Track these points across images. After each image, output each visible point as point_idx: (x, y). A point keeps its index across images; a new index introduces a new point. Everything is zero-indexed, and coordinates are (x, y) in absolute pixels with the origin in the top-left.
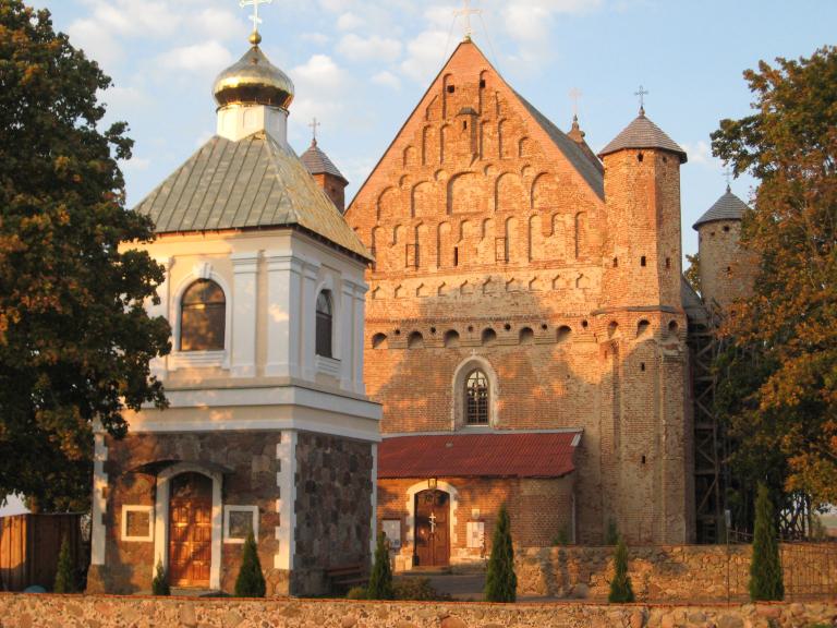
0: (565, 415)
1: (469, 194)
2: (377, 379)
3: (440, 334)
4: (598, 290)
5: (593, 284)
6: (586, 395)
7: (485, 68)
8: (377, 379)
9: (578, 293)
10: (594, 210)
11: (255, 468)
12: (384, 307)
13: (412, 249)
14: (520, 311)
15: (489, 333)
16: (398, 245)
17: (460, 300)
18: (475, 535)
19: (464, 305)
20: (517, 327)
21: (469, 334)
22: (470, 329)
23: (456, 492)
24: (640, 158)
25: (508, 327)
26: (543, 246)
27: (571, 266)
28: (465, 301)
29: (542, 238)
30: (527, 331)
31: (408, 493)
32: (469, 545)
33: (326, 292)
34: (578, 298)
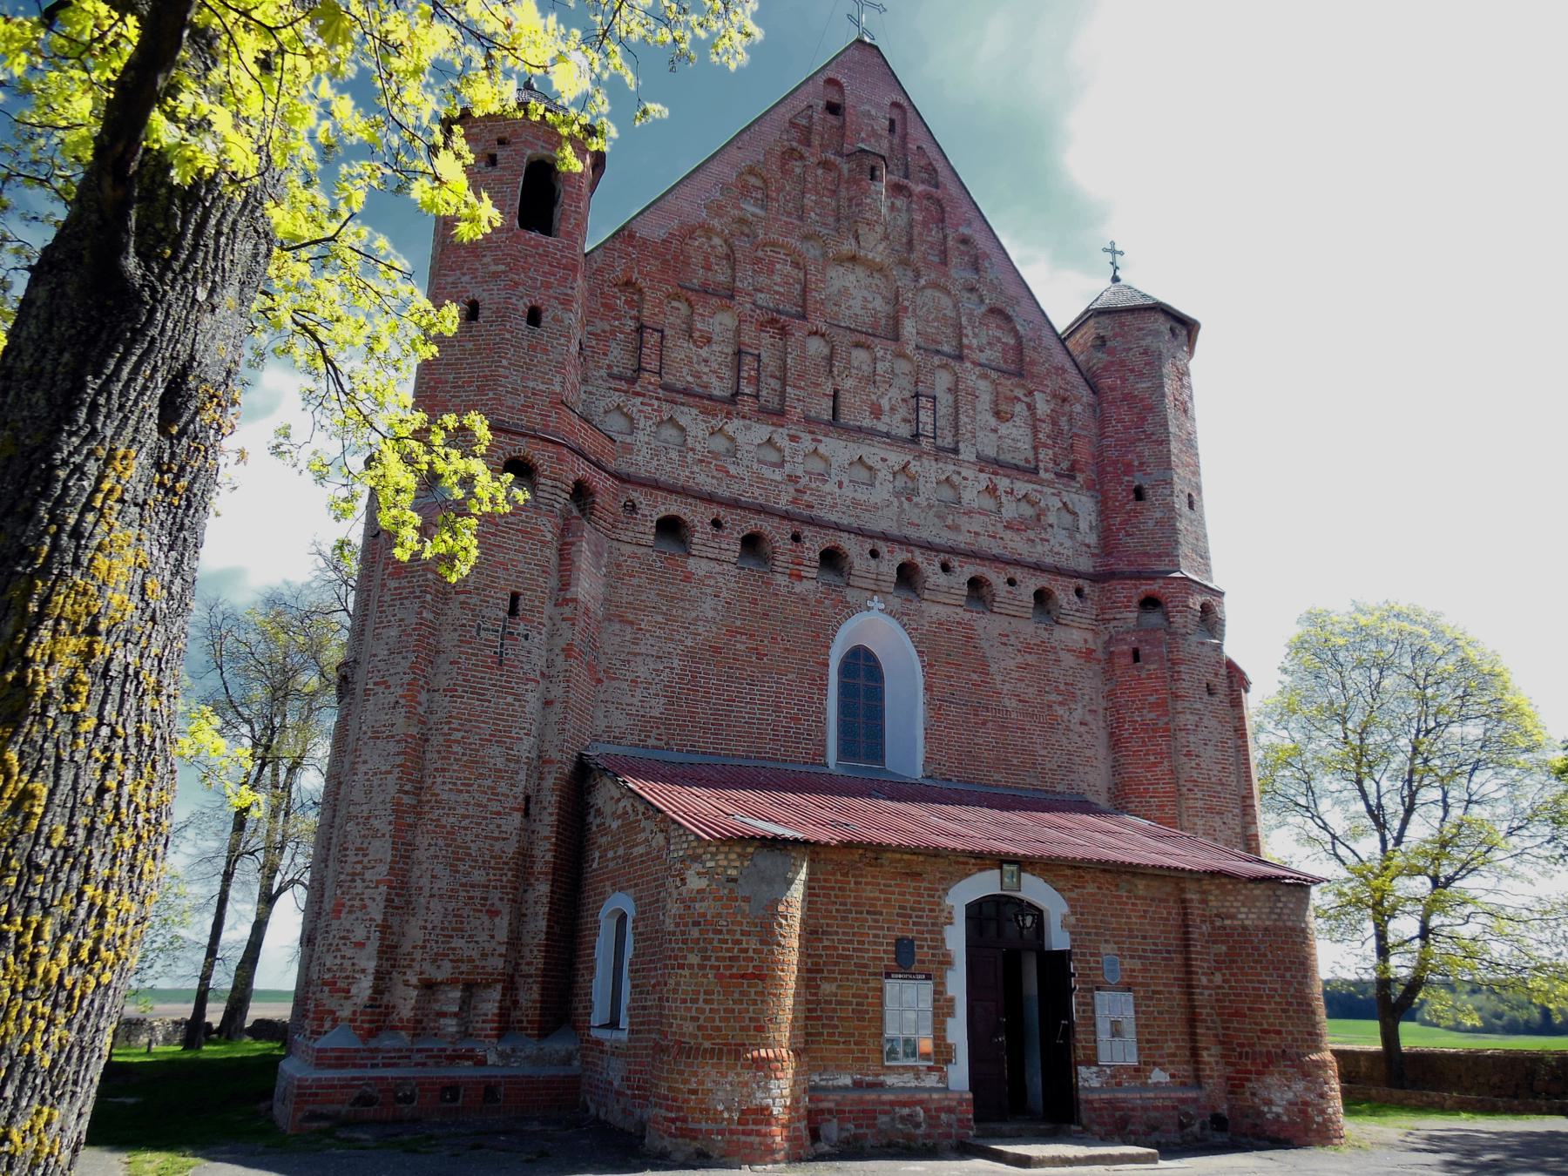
2: (660, 619)
4: (1092, 539)
8: (660, 619)
12: (684, 464)
15: (907, 576)
16: (715, 347)
17: (848, 491)
18: (1116, 1031)
19: (856, 503)
21: (873, 562)
23: (1065, 909)
25: (945, 568)
26: (993, 436)
27: (1050, 484)
28: (858, 496)
29: (993, 422)
31: (949, 901)
32: (1104, 1059)
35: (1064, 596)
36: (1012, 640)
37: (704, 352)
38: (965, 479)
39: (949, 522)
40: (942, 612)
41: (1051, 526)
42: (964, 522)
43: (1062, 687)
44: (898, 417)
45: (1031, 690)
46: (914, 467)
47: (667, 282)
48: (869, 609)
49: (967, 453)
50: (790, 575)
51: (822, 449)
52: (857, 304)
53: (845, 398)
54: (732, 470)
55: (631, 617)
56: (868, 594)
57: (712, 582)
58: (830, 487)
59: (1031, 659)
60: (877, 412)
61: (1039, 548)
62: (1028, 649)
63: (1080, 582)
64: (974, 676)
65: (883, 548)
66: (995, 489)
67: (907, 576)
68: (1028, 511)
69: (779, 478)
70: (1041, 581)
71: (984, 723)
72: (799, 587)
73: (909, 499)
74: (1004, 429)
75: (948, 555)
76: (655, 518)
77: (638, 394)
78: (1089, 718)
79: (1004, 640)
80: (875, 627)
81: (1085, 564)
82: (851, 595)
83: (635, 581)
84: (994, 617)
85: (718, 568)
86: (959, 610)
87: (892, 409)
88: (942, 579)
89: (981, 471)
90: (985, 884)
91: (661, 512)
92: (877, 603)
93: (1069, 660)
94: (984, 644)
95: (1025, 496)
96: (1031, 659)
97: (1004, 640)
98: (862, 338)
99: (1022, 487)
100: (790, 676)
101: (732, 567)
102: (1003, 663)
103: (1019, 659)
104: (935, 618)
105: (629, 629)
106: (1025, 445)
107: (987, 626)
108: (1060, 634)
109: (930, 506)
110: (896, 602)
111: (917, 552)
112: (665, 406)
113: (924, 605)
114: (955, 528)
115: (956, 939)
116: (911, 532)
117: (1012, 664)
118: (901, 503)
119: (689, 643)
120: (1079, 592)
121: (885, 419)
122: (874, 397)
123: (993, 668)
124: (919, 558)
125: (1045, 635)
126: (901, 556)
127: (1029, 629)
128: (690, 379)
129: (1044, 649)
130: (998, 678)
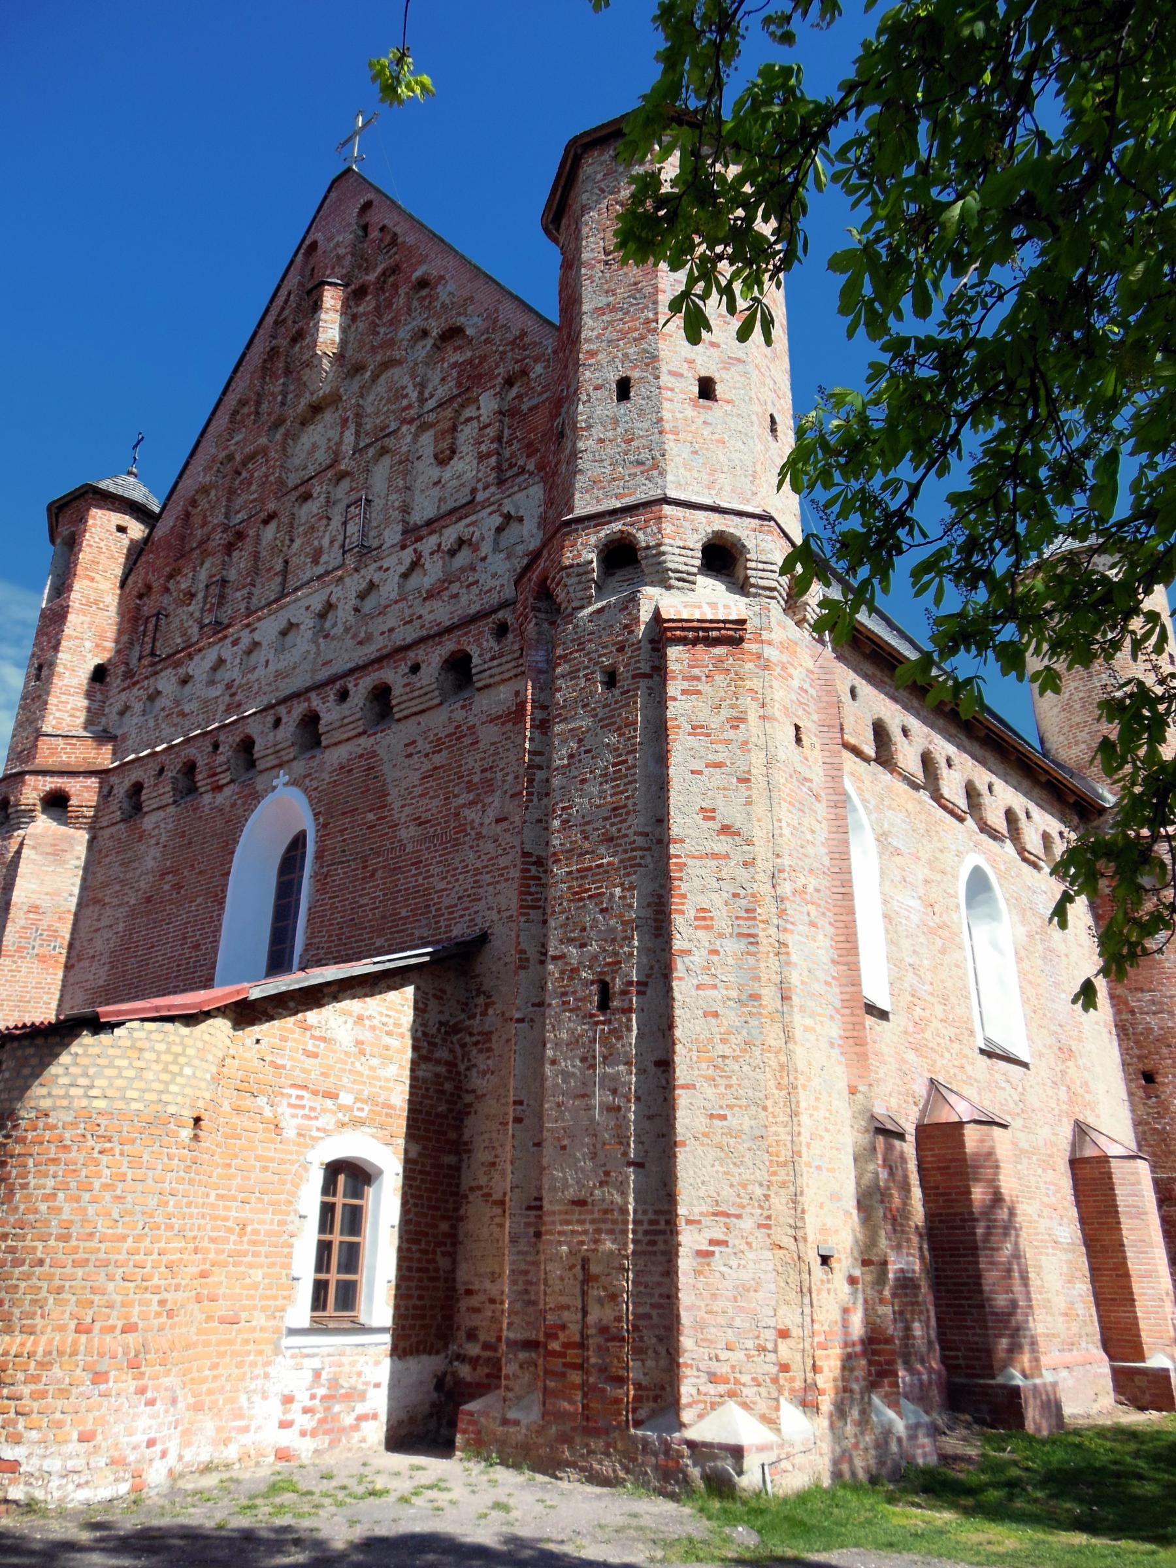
0: (447, 902)
1: (322, 450)
6: (499, 828)
7: (370, 196)
8: (118, 888)
10: (536, 360)
13: (215, 590)
14: (371, 650)
19: (279, 674)
22: (277, 723)
26: (436, 492)
27: (487, 503)
29: (435, 472)
34: (494, 576)
35: (480, 648)
36: (420, 743)
37: (191, 608)
38: (388, 569)
39: (362, 635)
41: (484, 559)
42: (379, 626)
43: (476, 779)
44: (337, 545)
45: (436, 802)
46: (337, 592)
47: (167, 565)
48: (274, 788)
50: (213, 790)
51: (257, 637)
53: (294, 561)
54: (187, 710)
55: (100, 895)
56: (274, 772)
57: (156, 832)
58: (260, 672)
59: (438, 759)
61: (464, 600)
62: (438, 745)
63: (500, 614)
64: (371, 816)
65: (282, 710)
66: (420, 557)
69: (219, 693)
70: (449, 645)
71: (375, 870)
72: (220, 799)
73: (326, 637)
74: (447, 475)
76: (122, 791)
77: (134, 684)
78: (511, 807)
79: (410, 750)
82: (260, 783)
83: (108, 860)
84: (401, 726)
85: (161, 814)
86: (362, 740)
87: (332, 542)
89: (404, 547)
91: (127, 784)
92: (283, 777)
94: (386, 768)
95: (461, 542)
96: (438, 759)
97: (410, 750)
98: (302, 489)
99: (450, 535)
100: (199, 900)
101: (172, 809)
102: (402, 777)
103: (427, 766)
104: (336, 766)
105: (97, 907)
109: (347, 630)
110: (299, 767)
111: (313, 695)
112: (152, 680)
113: (328, 752)
114: (369, 638)
117: (415, 778)
118: (318, 646)
119: (133, 902)
121: (322, 560)
122: (316, 543)
123: (394, 792)
124: (316, 702)
125: (459, 715)
126: (299, 709)
127: (439, 721)
128: (179, 640)
129: (457, 734)
130: (396, 805)
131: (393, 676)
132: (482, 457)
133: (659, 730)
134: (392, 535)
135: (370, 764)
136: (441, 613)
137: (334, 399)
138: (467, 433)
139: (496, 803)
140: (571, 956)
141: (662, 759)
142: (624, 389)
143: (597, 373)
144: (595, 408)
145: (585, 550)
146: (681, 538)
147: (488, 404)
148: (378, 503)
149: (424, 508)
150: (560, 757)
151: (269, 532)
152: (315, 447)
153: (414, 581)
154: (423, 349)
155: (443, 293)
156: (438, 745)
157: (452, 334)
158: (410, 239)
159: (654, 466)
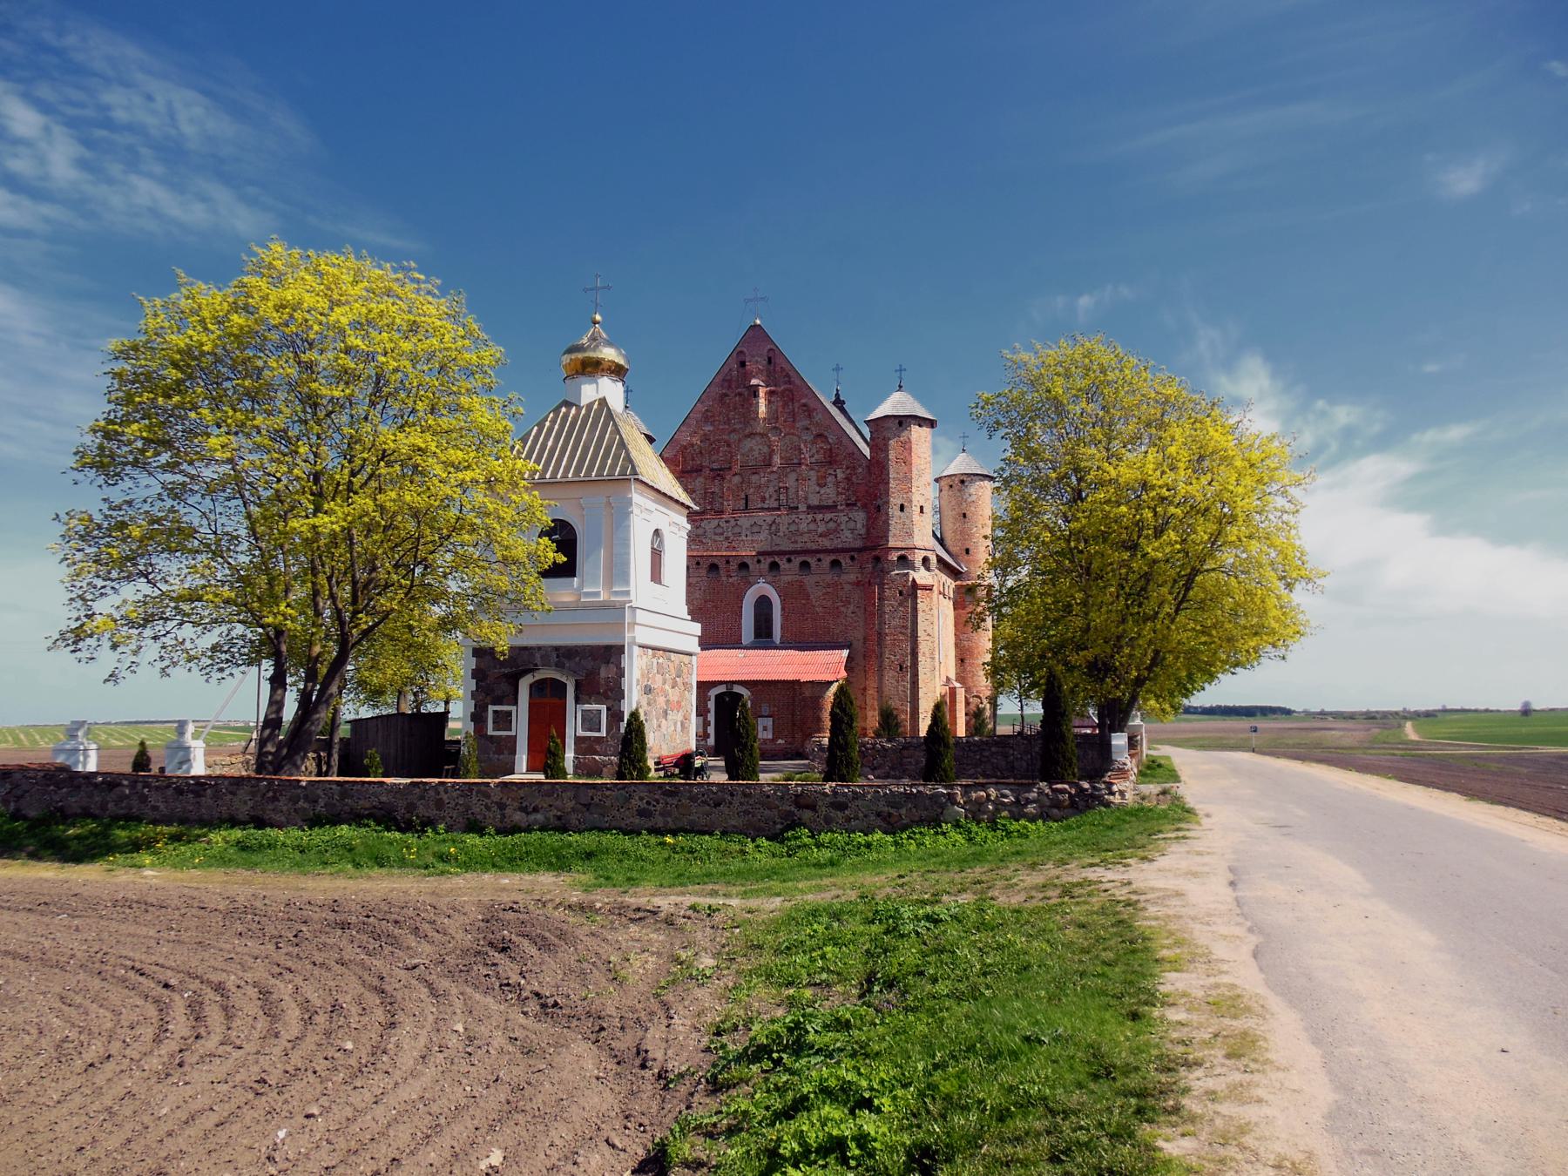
3: (734, 566)
4: (863, 531)
5: (859, 526)
9: (848, 533)
11: (603, 673)
14: (798, 546)
15: (774, 566)
18: (765, 729)
20: (797, 560)
24: (900, 424)
25: (789, 561)
30: (805, 565)
33: (657, 532)
35: (845, 560)
40: (789, 578)
42: (799, 539)
49: (802, 508)
52: (756, 454)
60: (763, 500)
62: (828, 586)
67: (774, 566)
68: (832, 525)
70: (833, 557)
75: (789, 555)
80: (762, 587)
81: (858, 544)
88: (787, 566)
90: (722, 689)
93: (847, 587)
99: (828, 516)
102: (816, 594)
106: (833, 495)
107: (809, 580)
108: (844, 577)
115: (711, 705)
116: (777, 549)
120: (852, 558)
126: (769, 560)
127: (828, 578)
131: (812, 561)
132: (839, 494)
133: (915, 610)
134: (802, 508)
135: (801, 585)
136: (826, 543)
137: (762, 435)
138: (830, 479)
139: (851, 608)
140: (890, 658)
141: (915, 616)
142: (902, 508)
143: (895, 501)
144: (894, 511)
145: (894, 556)
146: (918, 557)
147: (840, 475)
148: (792, 491)
149: (814, 501)
150: (887, 609)
151: (737, 479)
152: (751, 450)
153: (812, 526)
154: (809, 438)
155: (818, 417)
156: (828, 586)
157: (820, 435)
158: (798, 382)
159: (910, 534)
